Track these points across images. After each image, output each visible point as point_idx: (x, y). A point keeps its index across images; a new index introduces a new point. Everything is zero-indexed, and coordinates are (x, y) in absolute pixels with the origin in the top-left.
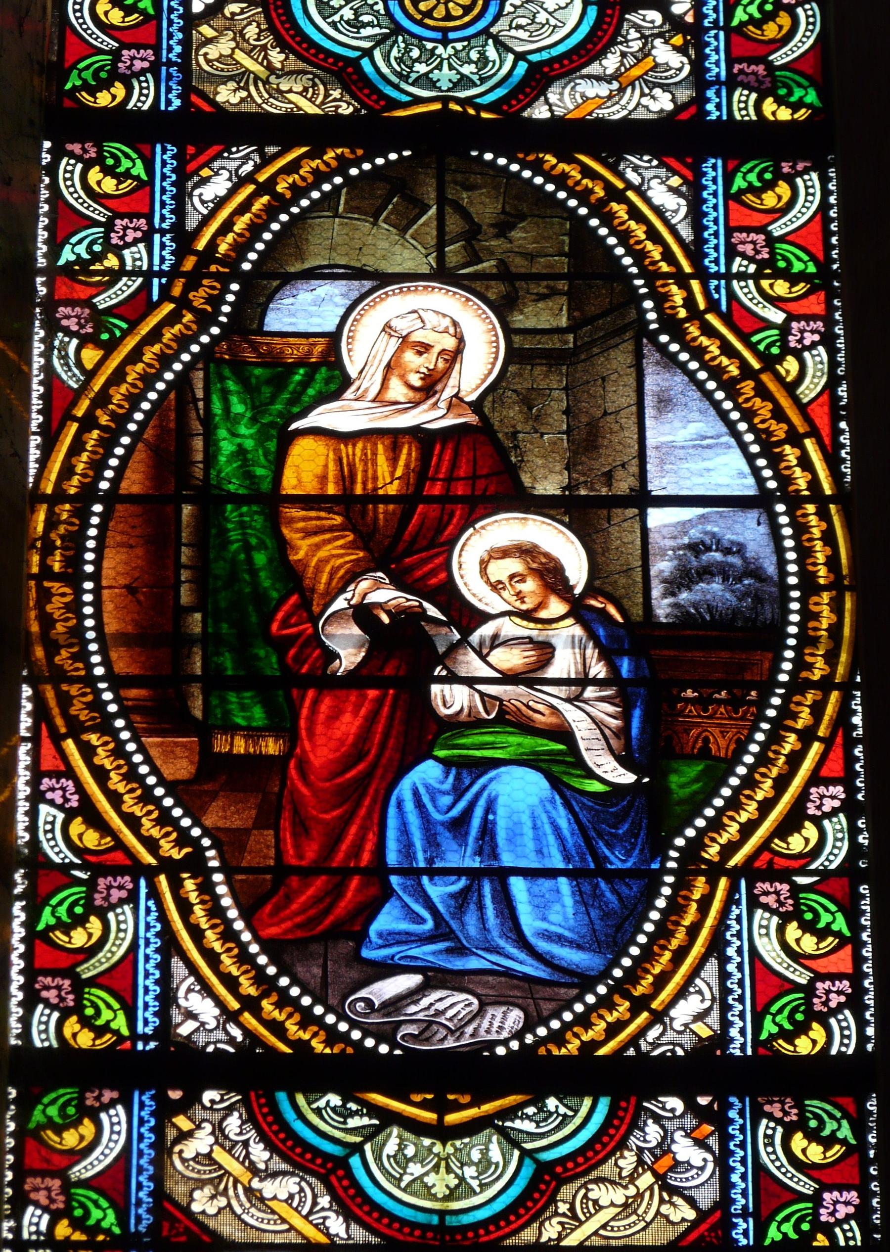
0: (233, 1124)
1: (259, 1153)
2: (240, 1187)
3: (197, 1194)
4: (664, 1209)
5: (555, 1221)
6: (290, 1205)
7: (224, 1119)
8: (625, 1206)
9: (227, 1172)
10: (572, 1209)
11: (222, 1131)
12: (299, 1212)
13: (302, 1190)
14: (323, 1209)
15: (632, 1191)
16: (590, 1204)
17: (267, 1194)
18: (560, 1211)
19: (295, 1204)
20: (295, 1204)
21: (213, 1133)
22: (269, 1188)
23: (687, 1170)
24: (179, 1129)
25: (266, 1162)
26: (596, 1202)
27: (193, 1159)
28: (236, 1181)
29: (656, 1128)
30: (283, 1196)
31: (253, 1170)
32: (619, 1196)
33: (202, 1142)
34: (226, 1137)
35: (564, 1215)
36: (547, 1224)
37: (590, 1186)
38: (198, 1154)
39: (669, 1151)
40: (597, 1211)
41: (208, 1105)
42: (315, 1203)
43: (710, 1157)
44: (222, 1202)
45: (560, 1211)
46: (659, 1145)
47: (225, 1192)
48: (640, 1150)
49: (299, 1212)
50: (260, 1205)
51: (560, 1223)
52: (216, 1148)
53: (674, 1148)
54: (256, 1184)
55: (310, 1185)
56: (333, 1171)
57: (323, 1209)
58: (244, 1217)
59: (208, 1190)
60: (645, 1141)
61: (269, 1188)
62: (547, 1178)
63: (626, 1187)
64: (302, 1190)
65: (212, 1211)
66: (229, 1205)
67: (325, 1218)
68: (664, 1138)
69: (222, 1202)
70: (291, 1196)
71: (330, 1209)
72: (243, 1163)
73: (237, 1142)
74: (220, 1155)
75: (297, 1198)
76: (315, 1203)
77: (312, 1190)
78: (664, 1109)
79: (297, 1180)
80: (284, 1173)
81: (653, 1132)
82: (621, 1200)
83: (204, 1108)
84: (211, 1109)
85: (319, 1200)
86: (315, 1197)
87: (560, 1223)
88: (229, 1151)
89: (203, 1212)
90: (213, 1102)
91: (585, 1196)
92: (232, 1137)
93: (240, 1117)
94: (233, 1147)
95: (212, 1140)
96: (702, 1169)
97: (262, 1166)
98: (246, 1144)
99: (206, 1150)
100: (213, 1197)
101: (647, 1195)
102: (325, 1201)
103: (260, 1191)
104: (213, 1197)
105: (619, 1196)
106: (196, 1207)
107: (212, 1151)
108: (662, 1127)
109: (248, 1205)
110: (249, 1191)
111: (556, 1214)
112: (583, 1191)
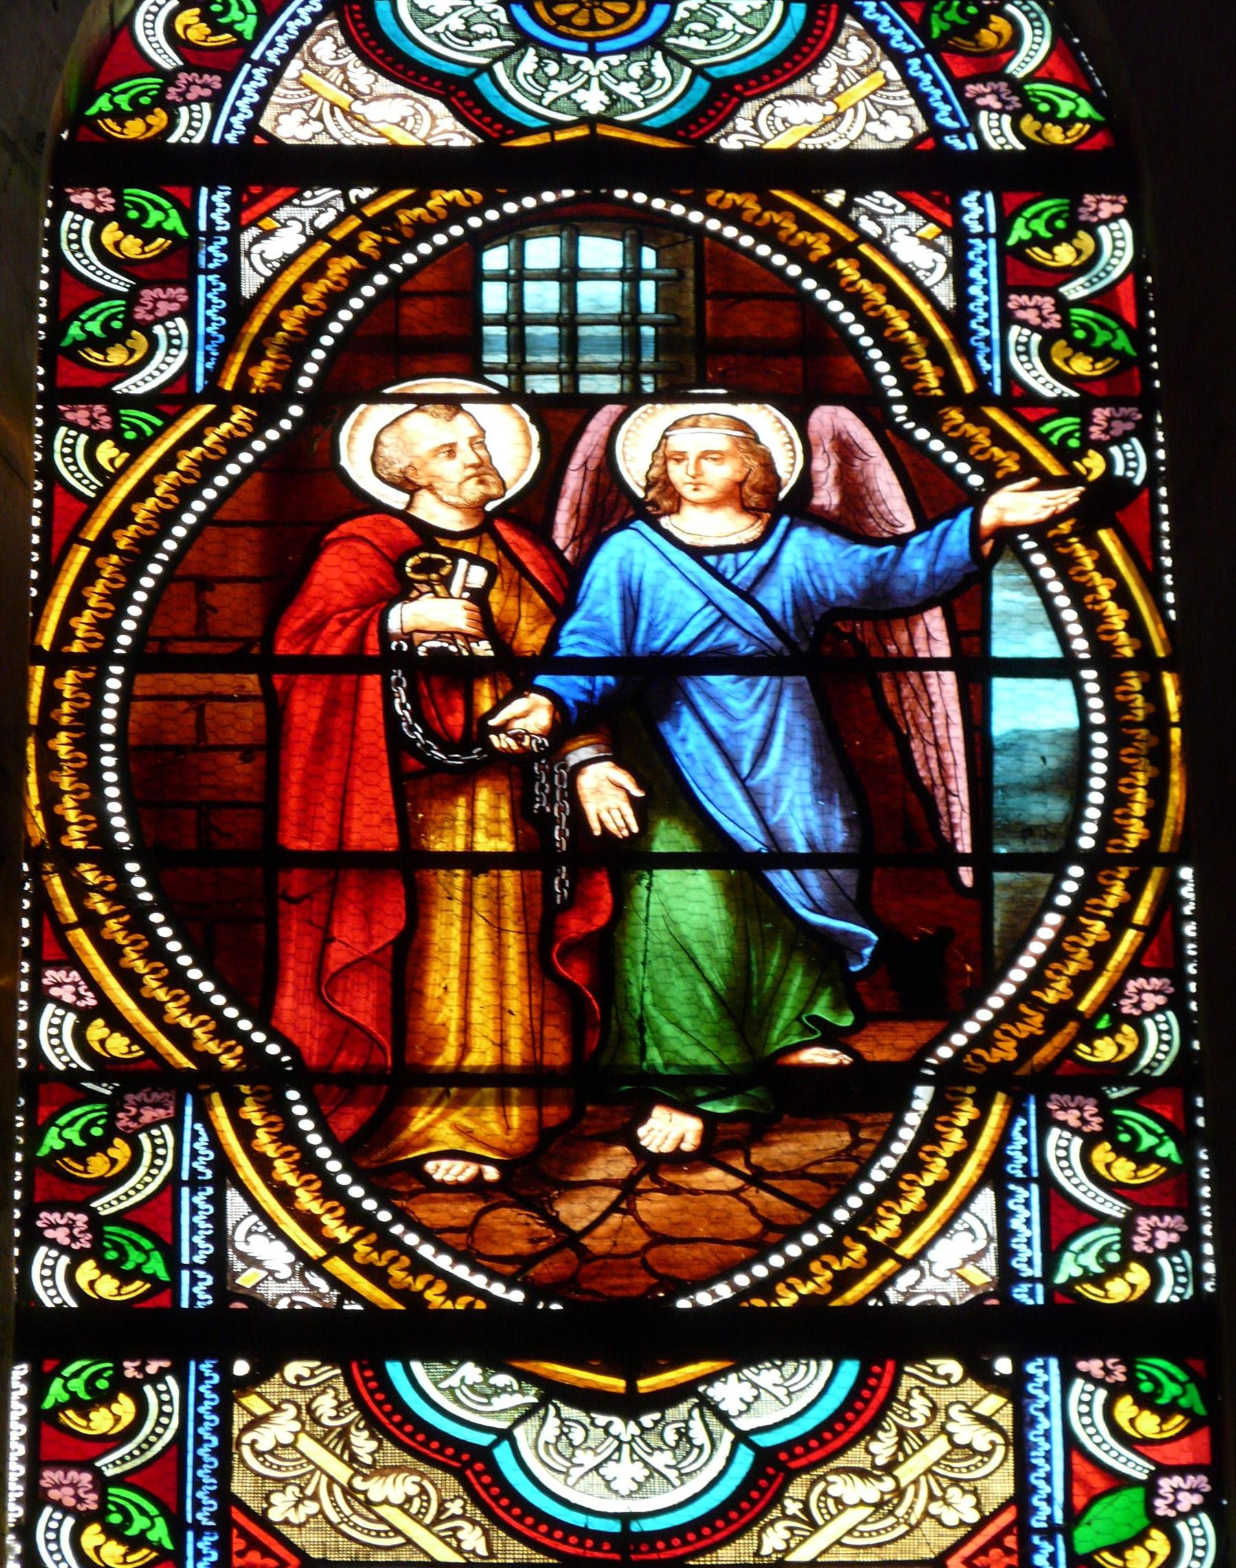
2: (337, 1490)
4: (935, 1508)
9: (318, 1467)
10: (806, 1510)
12: (420, 1522)
14: (453, 1517)
16: (831, 1502)
17: (373, 1497)
18: (789, 1512)
20: (414, 1510)
21: (298, 1418)
22: (376, 1489)
26: (838, 1501)
27: (271, 1452)
28: (332, 1480)
30: (398, 1498)
32: (871, 1491)
33: (283, 1427)
34: (317, 1421)
35: (794, 1518)
37: (830, 1478)
42: (442, 1509)
43: (999, 1439)
45: (789, 1512)
47: (315, 1497)
50: (364, 1511)
52: (302, 1436)
54: (358, 1483)
56: (469, 1465)
57: (453, 1517)
58: (343, 1527)
61: (376, 1489)
62: (770, 1471)
63: (879, 1478)
64: (424, 1491)
66: (321, 1511)
67: (455, 1530)
69: (311, 1507)
70: (409, 1499)
71: (462, 1517)
72: (340, 1457)
74: (306, 1444)
80: (397, 1469)
83: (285, 1382)
87: (790, 1529)
91: (824, 1493)
95: (297, 1426)
96: (989, 1454)
100: (299, 1501)
104: (299, 1501)
105: (871, 1491)
106: (275, 1515)
109: (348, 1511)
110: (349, 1491)
112: (821, 1486)
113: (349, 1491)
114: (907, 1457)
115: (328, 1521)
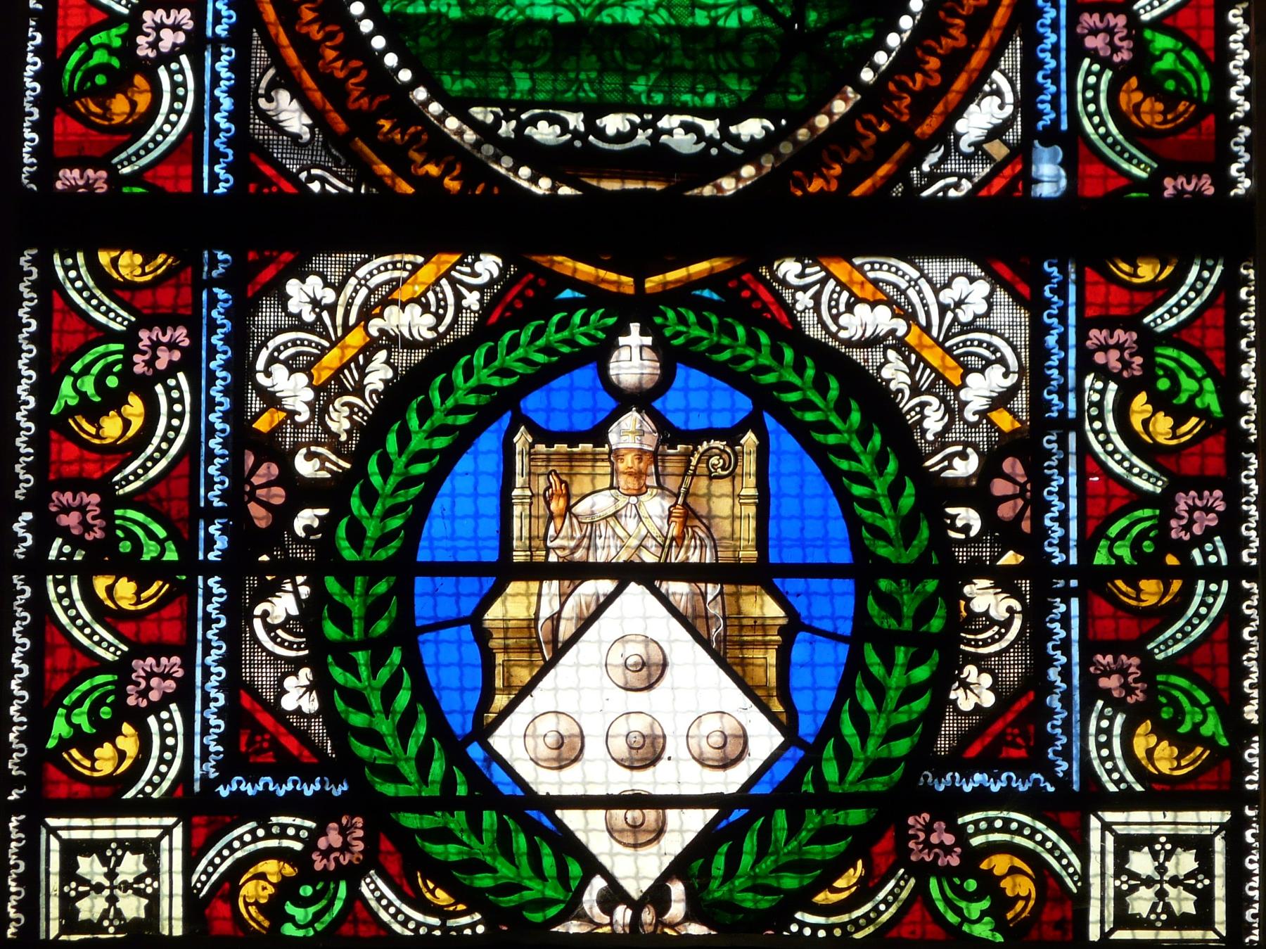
0: (934, 422)
1: (895, 373)
2: (923, 322)
3: (982, 308)
5: (485, 278)
6: (852, 294)
7: (947, 429)
8: (386, 302)
11: (949, 410)
12: (839, 283)
13: (835, 319)
15: (375, 326)
18: (476, 295)
19: (845, 295)
21: (964, 404)
22: (881, 319)
23: (294, 357)
24: (1011, 411)
25: (887, 361)
26: (426, 308)
29: (334, 427)
30: (861, 309)
31: (901, 346)
32: (396, 320)
33: (979, 390)
34: (943, 400)
35: (471, 288)
36: (496, 273)
38: (982, 371)
39: (317, 390)
40: (424, 294)
41: (970, 450)
42: (817, 298)
44: (947, 296)
45: (476, 295)
46: (330, 401)
47: (943, 309)
48: (359, 390)
49: (839, 283)
51: (475, 274)
52: (957, 382)
53: (309, 395)
54: (901, 326)
55: (825, 327)
57: (805, 288)
59: (965, 316)
60: (350, 405)
61: (881, 319)
63: (382, 331)
64: (835, 319)
65: (960, 284)
66: (936, 292)
68: (324, 411)
69: (947, 296)
70: (850, 308)
72: (920, 359)
73: (929, 391)
75: (842, 308)
76: (817, 298)
77: (821, 321)
78: (323, 459)
79: (843, 335)
81: (339, 422)
82: (392, 312)
83: (975, 446)
84: (966, 444)
85: (811, 304)
86: (817, 308)
88: (939, 376)
89: (972, 280)
90: (964, 456)
91: (440, 319)
92: (935, 402)
93: (924, 432)
94: (932, 385)
97: (891, 354)
98: (915, 390)
99: (973, 379)
100: (960, 303)
101: (352, 320)
102: (804, 300)
103: (894, 316)
104: (960, 303)
105: (396, 320)
106: (983, 287)
107: (963, 377)
108: (327, 430)
109: (912, 293)
110: (910, 317)
111: (480, 288)
113: (910, 317)
114: (354, 358)
115: (929, 281)
